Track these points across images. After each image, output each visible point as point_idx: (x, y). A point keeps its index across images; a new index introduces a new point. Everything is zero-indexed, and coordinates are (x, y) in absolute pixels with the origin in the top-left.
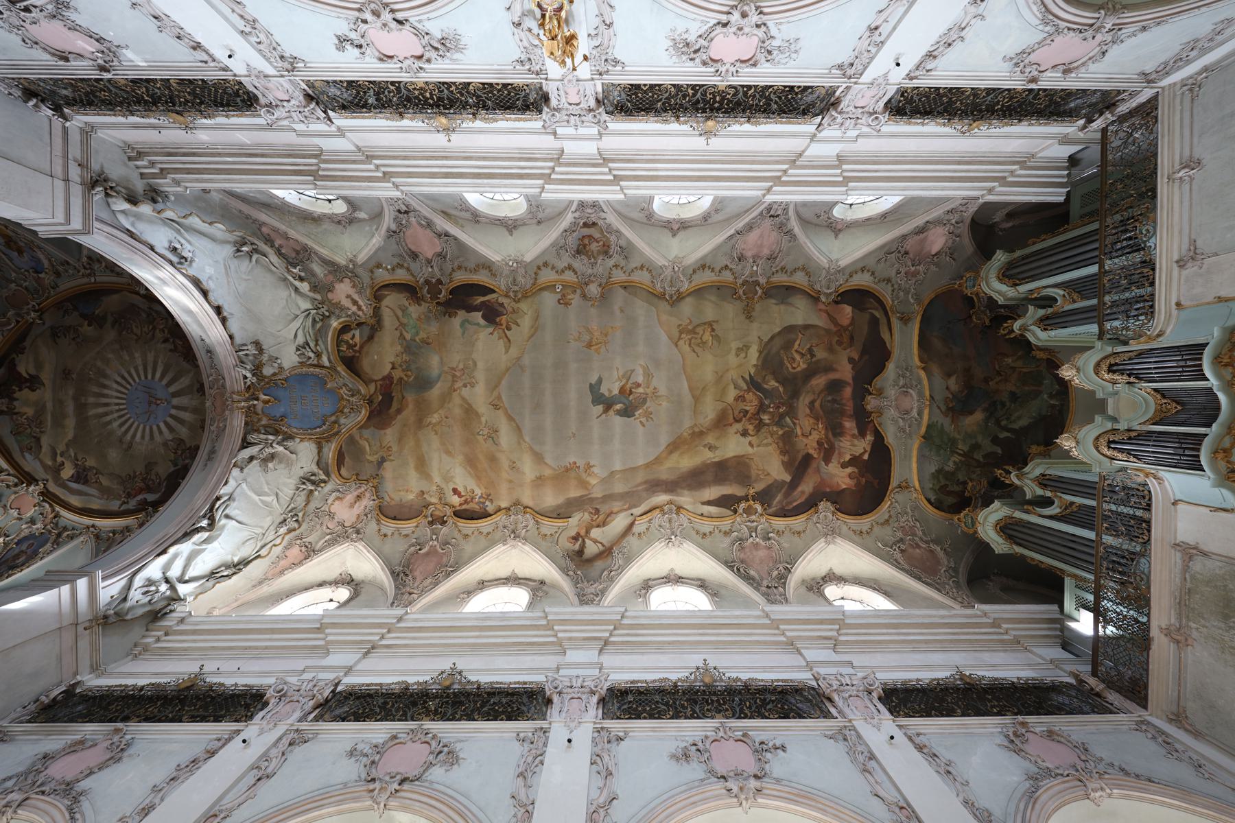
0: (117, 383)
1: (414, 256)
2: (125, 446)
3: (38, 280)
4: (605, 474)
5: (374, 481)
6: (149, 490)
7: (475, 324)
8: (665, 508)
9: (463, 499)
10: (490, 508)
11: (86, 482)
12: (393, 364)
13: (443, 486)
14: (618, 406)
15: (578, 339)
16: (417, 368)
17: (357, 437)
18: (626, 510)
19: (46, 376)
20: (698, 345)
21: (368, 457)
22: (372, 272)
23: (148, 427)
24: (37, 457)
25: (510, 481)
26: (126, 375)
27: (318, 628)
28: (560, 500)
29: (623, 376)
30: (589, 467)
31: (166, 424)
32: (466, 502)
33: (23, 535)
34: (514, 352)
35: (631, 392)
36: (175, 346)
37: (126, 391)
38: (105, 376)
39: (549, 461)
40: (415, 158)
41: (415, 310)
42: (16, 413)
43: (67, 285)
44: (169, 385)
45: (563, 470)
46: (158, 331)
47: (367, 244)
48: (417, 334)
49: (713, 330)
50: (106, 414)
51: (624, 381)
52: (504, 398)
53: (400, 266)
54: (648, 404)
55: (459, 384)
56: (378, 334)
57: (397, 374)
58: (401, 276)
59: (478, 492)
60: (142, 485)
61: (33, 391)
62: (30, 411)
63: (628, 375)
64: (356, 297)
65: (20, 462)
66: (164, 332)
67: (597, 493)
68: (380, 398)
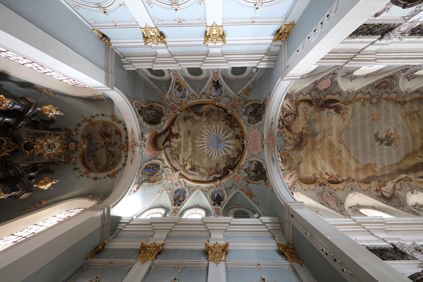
0: (206, 135)
1: (317, 90)
2: (209, 158)
3: (181, 101)
4: (381, 167)
5: (297, 169)
6: (217, 173)
7: (331, 113)
8: (405, 179)
9: (330, 176)
10: (340, 180)
11: (195, 170)
12: (303, 128)
13: (322, 171)
14: (385, 142)
15: (369, 118)
16: (311, 129)
17: (291, 154)
18: (391, 180)
19: (182, 133)
20: (413, 120)
21: (295, 161)
22: (298, 96)
23: (217, 151)
24: (178, 162)
25: (347, 170)
26: (210, 133)
27: (357, 224)
28: (365, 177)
29: (386, 131)
30: (375, 164)
31: (224, 150)
32: (331, 177)
33: (175, 190)
34: (346, 123)
35: (389, 137)
36: (227, 123)
37: (210, 139)
38: (203, 133)
39: (360, 162)
40: (391, 53)
41: (310, 109)
42: (171, 147)
43: (191, 102)
44: (225, 136)
45: (366, 165)
46: (221, 117)
47: (301, 86)
48: (311, 117)
49: (418, 114)
50: (203, 146)
51: (387, 133)
52: (343, 139)
53: (308, 93)
54: (396, 141)
55: (327, 135)
56: (297, 117)
57: (304, 131)
58: (308, 97)
59: (335, 174)
60: (215, 171)
61: (177, 139)
62: (176, 146)
63: (388, 131)
64: (290, 105)
65: (172, 164)
66: (223, 118)
67: (379, 174)
68: (299, 140)
